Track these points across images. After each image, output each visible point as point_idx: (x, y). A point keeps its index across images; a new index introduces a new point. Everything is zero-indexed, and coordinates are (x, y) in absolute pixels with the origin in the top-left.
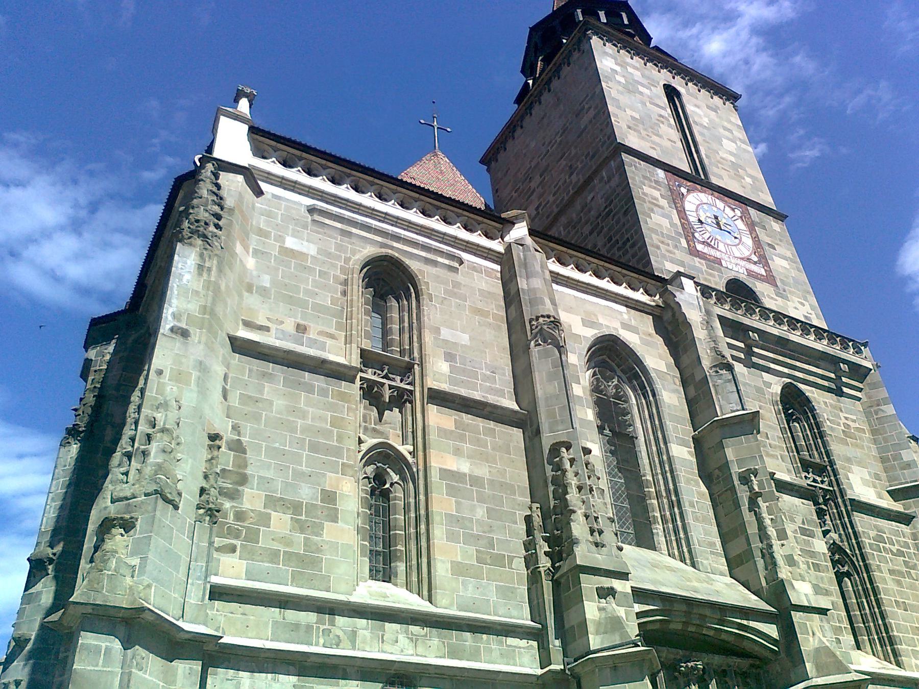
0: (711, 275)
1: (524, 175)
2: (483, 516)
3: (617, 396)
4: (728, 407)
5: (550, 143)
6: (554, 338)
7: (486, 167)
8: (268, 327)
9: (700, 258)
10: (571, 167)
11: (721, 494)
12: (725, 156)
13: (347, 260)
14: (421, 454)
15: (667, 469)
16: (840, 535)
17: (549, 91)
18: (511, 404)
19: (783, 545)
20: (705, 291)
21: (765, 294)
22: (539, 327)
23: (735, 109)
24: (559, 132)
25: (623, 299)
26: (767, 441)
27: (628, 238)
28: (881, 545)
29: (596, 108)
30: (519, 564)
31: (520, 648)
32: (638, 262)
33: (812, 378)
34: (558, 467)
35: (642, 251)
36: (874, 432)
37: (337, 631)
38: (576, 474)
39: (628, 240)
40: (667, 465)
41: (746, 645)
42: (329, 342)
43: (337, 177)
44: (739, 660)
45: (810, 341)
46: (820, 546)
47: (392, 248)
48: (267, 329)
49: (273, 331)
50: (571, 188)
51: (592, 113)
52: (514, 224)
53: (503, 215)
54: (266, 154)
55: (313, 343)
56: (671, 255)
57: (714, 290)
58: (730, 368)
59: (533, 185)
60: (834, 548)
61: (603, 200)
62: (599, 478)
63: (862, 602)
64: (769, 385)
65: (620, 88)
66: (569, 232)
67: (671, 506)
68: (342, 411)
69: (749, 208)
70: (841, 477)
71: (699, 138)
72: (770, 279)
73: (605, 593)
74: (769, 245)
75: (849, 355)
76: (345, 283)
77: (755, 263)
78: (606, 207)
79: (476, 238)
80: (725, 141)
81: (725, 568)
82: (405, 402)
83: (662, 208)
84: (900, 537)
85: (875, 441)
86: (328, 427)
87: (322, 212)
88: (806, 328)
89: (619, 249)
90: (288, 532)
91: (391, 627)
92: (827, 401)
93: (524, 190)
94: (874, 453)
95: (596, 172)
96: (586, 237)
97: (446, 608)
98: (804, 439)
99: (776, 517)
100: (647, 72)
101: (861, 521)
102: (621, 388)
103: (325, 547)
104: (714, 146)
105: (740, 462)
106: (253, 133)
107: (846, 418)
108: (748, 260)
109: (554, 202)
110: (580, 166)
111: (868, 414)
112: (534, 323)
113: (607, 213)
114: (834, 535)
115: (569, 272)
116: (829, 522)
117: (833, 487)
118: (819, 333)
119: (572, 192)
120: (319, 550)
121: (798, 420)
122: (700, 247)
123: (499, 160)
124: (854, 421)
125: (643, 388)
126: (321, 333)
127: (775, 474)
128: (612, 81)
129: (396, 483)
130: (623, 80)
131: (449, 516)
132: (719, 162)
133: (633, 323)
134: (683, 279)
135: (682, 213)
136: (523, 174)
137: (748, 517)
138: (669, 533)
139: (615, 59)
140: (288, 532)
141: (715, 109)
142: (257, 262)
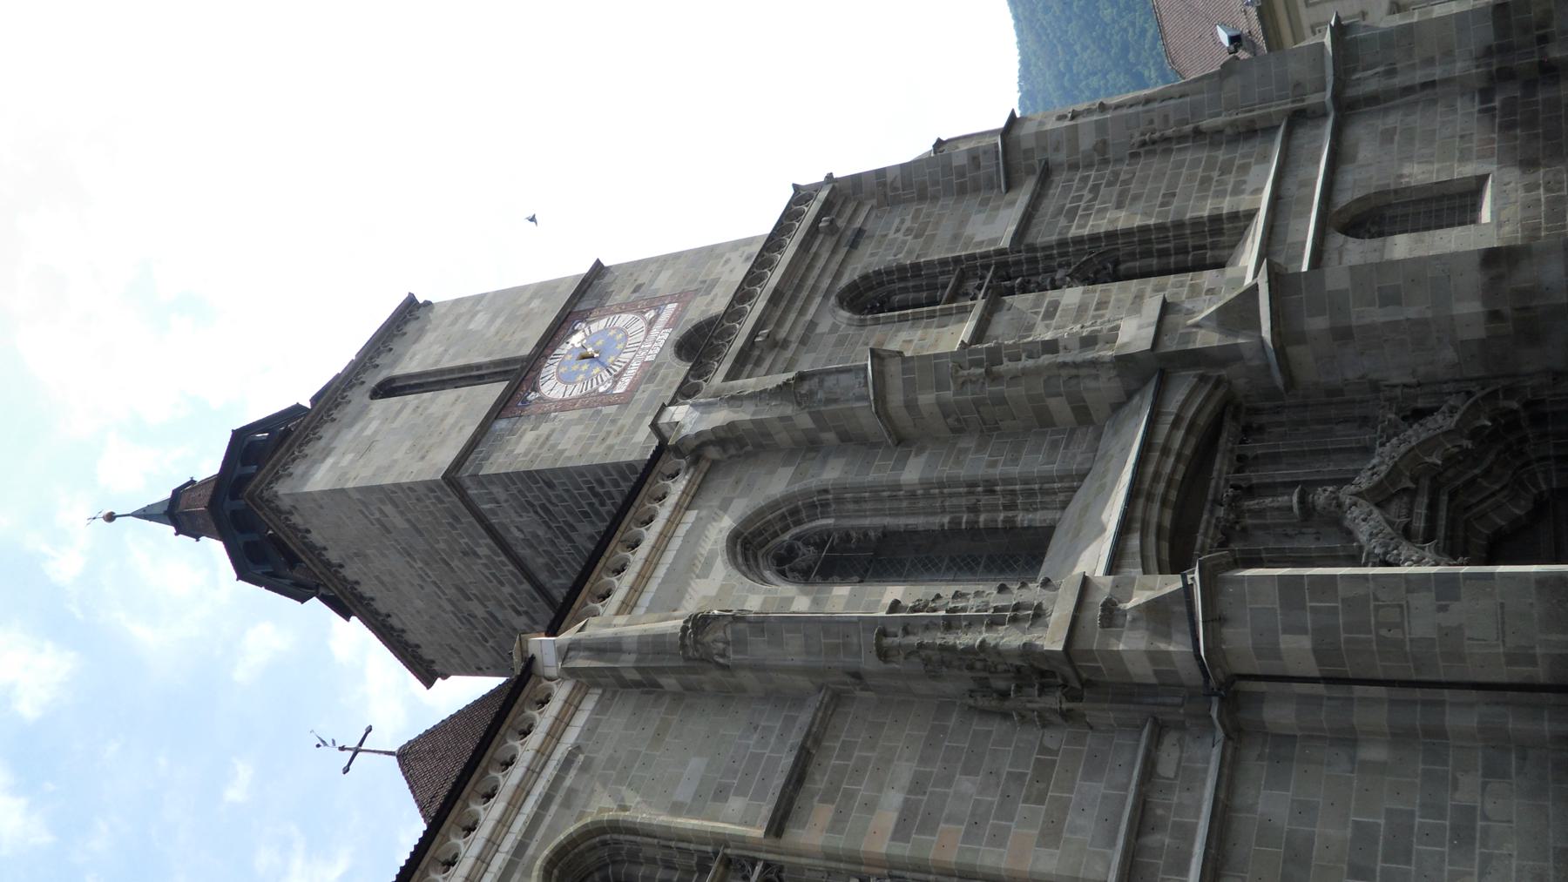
0: (663, 379)
1: (463, 623)
3: (820, 546)
4: (858, 390)
7: (439, 680)
10: (465, 554)
12: (493, 329)
15: (937, 491)
16: (1060, 266)
17: (341, 566)
19: (1065, 348)
20: (685, 392)
21: (704, 308)
24: (408, 562)
26: (915, 342)
27: (589, 488)
28: (1080, 213)
29: (381, 501)
31: (1180, 759)
32: (626, 479)
33: (834, 266)
35: (614, 473)
36: (922, 197)
39: (591, 489)
41: (1202, 421)
44: (1225, 435)
50: (496, 558)
51: (389, 509)
52: (533, 658)
56: (625, 431)
58: (802, 377)
59: (480, 612)
61: (524, 514)
62: (938, 596)
63: (1158, 250)
64: (834, 328)
65: (362, 462)
66: (564, 572)
67: (993, 492)
69: (576, 309)
71: (461, 362)
77: (657, 316)
78: (536, 512)
79: (544, 720)
80: (472, 326)
83: (553, 431)
85: (935, 198)
89: (603, 504)
92: (869, 252)
93: (486, 628)
96: (575, 547)
97: (1109, 868)
99: (1024, 351)
101: (1044, 235)
105: (940, 386)
107: (898, 230)
108: (651, 323)
109: (513, 585)
110: (466, 540)
113: (544, 512)
116: (1040, 278)
119: (503, 558)
121: (890, 294)
122: (621, 388)
123: (432, 658)
124: (903, 221)
125: (813, 506)
127: (962, 341)
128: (346, 473)
130: (349, 457)
131: (967, 837)
134: (665, 419)
135: (565, 405)
136: (460, 625)
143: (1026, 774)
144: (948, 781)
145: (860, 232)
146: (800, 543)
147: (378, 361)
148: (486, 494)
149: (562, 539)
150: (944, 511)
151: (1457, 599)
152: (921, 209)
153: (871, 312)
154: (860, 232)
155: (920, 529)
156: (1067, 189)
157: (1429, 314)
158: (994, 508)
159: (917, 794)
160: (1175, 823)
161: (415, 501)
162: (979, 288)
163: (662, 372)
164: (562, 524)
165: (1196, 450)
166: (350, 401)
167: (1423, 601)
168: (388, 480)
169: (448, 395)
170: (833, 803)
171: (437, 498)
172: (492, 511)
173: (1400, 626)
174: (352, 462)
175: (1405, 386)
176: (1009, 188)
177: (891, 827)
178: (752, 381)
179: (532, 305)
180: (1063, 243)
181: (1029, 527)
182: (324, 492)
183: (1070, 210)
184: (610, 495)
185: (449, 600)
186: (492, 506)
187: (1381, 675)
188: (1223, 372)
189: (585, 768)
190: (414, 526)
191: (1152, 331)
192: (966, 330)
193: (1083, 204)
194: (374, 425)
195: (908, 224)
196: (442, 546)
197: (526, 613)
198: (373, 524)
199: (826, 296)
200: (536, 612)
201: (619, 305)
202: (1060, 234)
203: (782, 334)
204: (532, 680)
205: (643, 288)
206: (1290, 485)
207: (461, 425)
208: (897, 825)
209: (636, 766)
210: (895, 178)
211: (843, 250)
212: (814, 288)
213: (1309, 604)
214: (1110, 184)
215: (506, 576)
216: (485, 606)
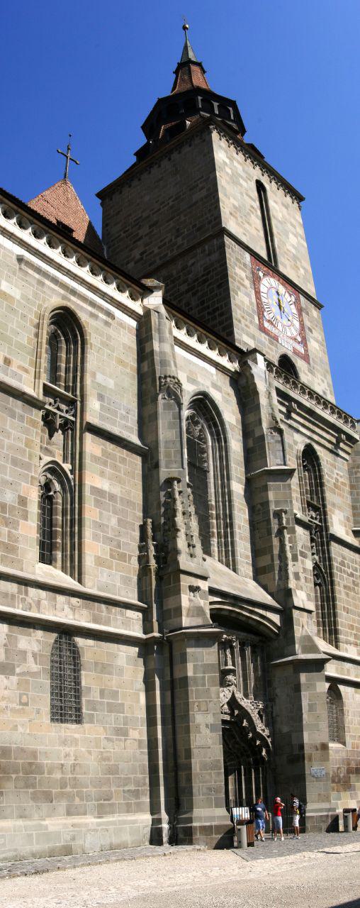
1: (136, 220)
2: (115, 525)
6: (176, 395)
10: (178, 230)
13: (40, 306)
14: (77, 472)
16: (320, 558)
17: (170, 159)
18: (135, 439)
20: (269, 365)
24: (172, 197)
28: (343, 568)
32: (224, 329)
34: (170, 496)
36: (352, 487)
37: (29, 600)
38: (183, 503)
39: (217, 309)
40: (226, 495)
41: (261, 627)
42: (25, 375)
44: (253, 637)
45: (326, 414)
46: (309, 565)
47: (69, 300)
51: (204, 193)
52: (152, 292)
55: (15, 375)
57: (275, 366)
58: (280, 432)
59: (141, 232)
60: (316, 567)
61: (202, 269)
64: (296, 443)
65: (227, 178)
67: (226, 527)
69: (300, 295)
70: (328, 517)
72: (306, 358)
73: (194, 589)
74: (309, 328)
75: (346, 429)
76: (38, 326)
77: (299, 343)
78: (203, 276)
79: (124, 298)
80: (291, 236)
81: (251, 574)
82: (68, 429)
83: (246, 288)
85: (351, 494)
86: (23, 446)
88: (326, 404)
89: (209, 313)
91: (61, 599)
94: (349, 502)
95: (200, 244)
100: (246, 168)
103: (20, 539)
105: (277, 503)
107: (337, 474)
111: (350, 473)
115: (181, 334)
118: (334, 409)
119: (175, 252)
120: (16, 541)
121: (308, 470)
122: (266, 325)
124: (341, 477)
125: (218, 434)
126: (20, 367)
130: (229, 171)
131: (95, 522)
132: (285, 252)
133: (219, 384)
135: (258, 293)
136: (134, 219)
138: (221, 545)
139: (226, 152)
141: (287, 207)
143: (120, 549)
144: (115, 512)
145: (338, 455)
146: (200, 428)
147: (273, 182)
149: (186, 288)
150: (216, 502)
151: (211, 732)
152: (346, 486)
153: (303, 462)
154: (338, 455)
155: (209, 490)
156: (353, 561)
157: (304, 722)
158: (218, 527)
160: (109, 617)
163: (274, 348)
165: (250, 625)
167: (210, 719)
168: (221, 195)
169: (258, 223)
172: (204, 251)
173: (199, 710)
174: (227, 173)
175: (272, 712)
176: (354, 532)
177: (96, 486)
179: (301, 269)
180: (330, 559)
181: (210, 544)
182: (213, 159)
183: (344, 562)
184: (214, 318)
185: (148, 217)
186: (207, 252)
187: (177, 702)
188: (281, 637)
189: (107, 323)
191: (302, 606)
192: (298, 516)
193: (346, 569)
194: (244, 183)
195: (340, 480)
196: (183, 218)
197: (142, 259)
198: (195, 182)
199: (309, 438)
201: (302, 321)
202: (335, 558)
203: (294, 415)
204: (141, 291)
206: (234, 665)
207: (247, 234)
208: (97, 488)
209: (109, 352)
211: (330, 446)
212: (313, 432)
213: (206, 675)
214: (354, 582)
216: (145, 236)
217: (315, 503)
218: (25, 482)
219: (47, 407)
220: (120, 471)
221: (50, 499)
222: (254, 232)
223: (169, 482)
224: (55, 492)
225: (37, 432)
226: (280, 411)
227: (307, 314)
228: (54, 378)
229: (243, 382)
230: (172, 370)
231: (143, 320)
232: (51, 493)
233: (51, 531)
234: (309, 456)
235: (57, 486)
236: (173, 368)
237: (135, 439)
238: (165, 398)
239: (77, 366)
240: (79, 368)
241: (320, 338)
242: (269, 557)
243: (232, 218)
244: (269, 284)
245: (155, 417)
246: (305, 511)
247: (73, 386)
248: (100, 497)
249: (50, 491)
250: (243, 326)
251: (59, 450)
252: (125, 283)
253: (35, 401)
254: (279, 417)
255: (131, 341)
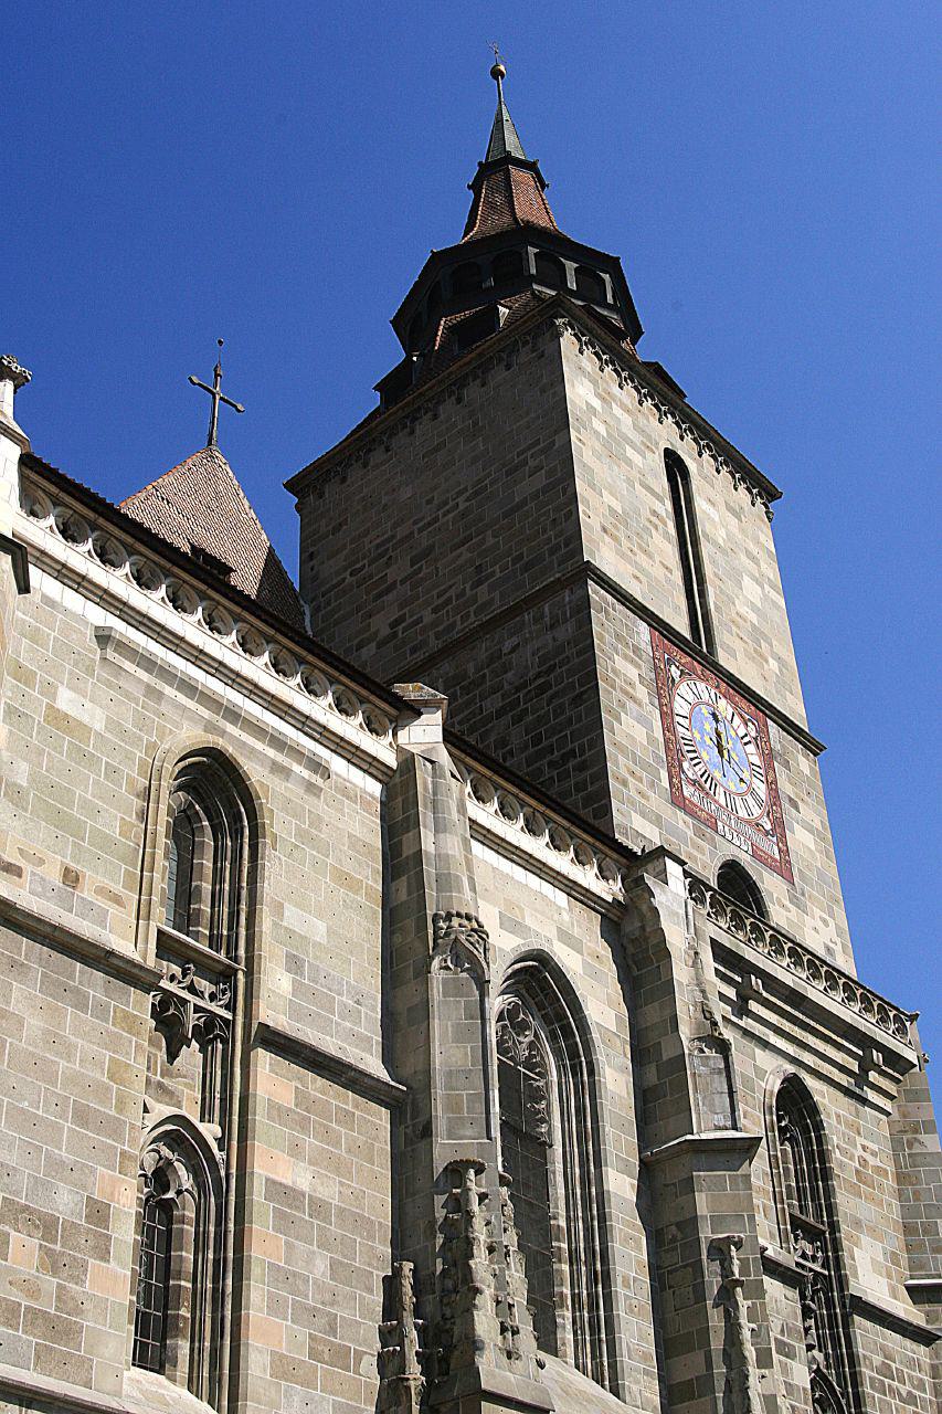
0: (698, 847)
1: (378, 546)
5: (446, 503)
8: (20, 868)
9: (686, 813)
10: (479, 569)
11: (676, 1270)
12: (744, 610)
14: (235, 1143)
17: (459, 400)
18: (375, 1067)
19: (763, 1377)
20: (696, 885)
21: (775, 896)
22: (453, 937)
23: (768, 518)
24: (466, 489)
25: (567, 883)
27: (573, 750)
30: (369, 1365)
32: (587, 801)
34: (459, 1205)
35: (596, 786)
36: (901, 1178)
42: (113, 909)
43: (147, 575)
45: (833, 1003)
46: (802, 1377)
47: (223, 733)
48: (18, 872)
49: (27, 876)
50: (472, 609)
51: (540, 480)
53: (398, 688)
54: (37, 508)
57: (711, 889)
58: (723, 1047)
59: (395, 573)
60: (819, 1379)
64: (761, 1073)
65: (598, 446)
67: (593, 1279)
68: (127, 1053)
69: (769, 722)
72: (784, 869)
74: (791, 799)
76: (146, 794)
78: (538, 676)
79: (350, 728)
80: (746, 581)
82: (215, 1038)
83: (640, 705)
84: (915, 1371)
85: (900, 1195)
87: (125, 648)
88: (833, 977)
89: (551, 764)
90: (33, 1272)
93: (371, 577)
94: (896, 1214)
98: (796, 1176)
99: (759, 1326)
100: (642, 421)
102: (538, 1049)
104: (729, 587)
105: (717, 1222)
106: (26, 465)
107: (864, 1148)
109: (434, 624)
111: (896, 1144)
112: (441, 924)
114: (815, 1352)
115: (486, 814)
117: (829, 1271)
120: (78, 1311)
122: (688, 791)
124: (874, 1154)
125: (574, 1055)
126: (100, 891)
129: (187, 1190)
130: (602, 429)
133: (576, 932)
134: (673, 868)
135: (667, 716)
137: (716, 1319)
139: (595, 383)
140: (33, 1272)
141: (737, 515)
142: (10, 731)
145: (864, 1101)
147: (706, 455)
148: (564, 613)
150: (568, 1218)
154: (864, 1101)
156: (914, 1364)
159: (310, 1207)
161: (552, 517)
162: (804, 1256)
164: (522, 706)
166: (661, 423)
170: (296, 1105)
171: (557, 548)
172: (538, 619)
174: (596, 432)
176: (909, 1289)
178: (710, 975)
179: (770, 660)
180: (853, 1360)
186: (547, 619)
189: (311, 788)
190: (519, 506)
192: (770, 1253)
194: (636, 459)
195: (872, 1161)
196: (491, 541)
197: (395, 635)
200: (396, 648)
201: (775, 782)
203: (754, 1006)
204: (393, 712)
205: (794, 811)
210: (922, 1143)
211: (844, 1080)
215: (448, 615)
216: (403, 582)
217: (811, 1220)
218: (104, 1166)
219: (164, 984)
220: (337, 1144)
221: (167, 1207)
222: (659, 572)
223: (457, 1170)
224: (179, 1193)
225: (140, 1044)
226: (722, 997)
227: (787, 765)
228: (184, 914)
229: (631, 926)
230: (463, 900)
231: (397, 779)
232: (171, 1195)
233: (167, 1288)
234: (794, 1103)
235: (185, 1179)
236: (468, 894)
237: (375, 1067)
238: (447, 968)
239: (240, 888)
240: (244, 893)
241: (817, 824)
242: (700, 1356)
243: (607, 539)
244: (693, 694)
245: (423, 1011)
246: (788, 1242)
247: (228, 936)
248: (290, 1206)
249: (167, 1190)
250: (633, 793)
251: (192, 1088)
252: (353, 691)
253: (136, 971)
254: (720, 1010)
255: (370, 831)
